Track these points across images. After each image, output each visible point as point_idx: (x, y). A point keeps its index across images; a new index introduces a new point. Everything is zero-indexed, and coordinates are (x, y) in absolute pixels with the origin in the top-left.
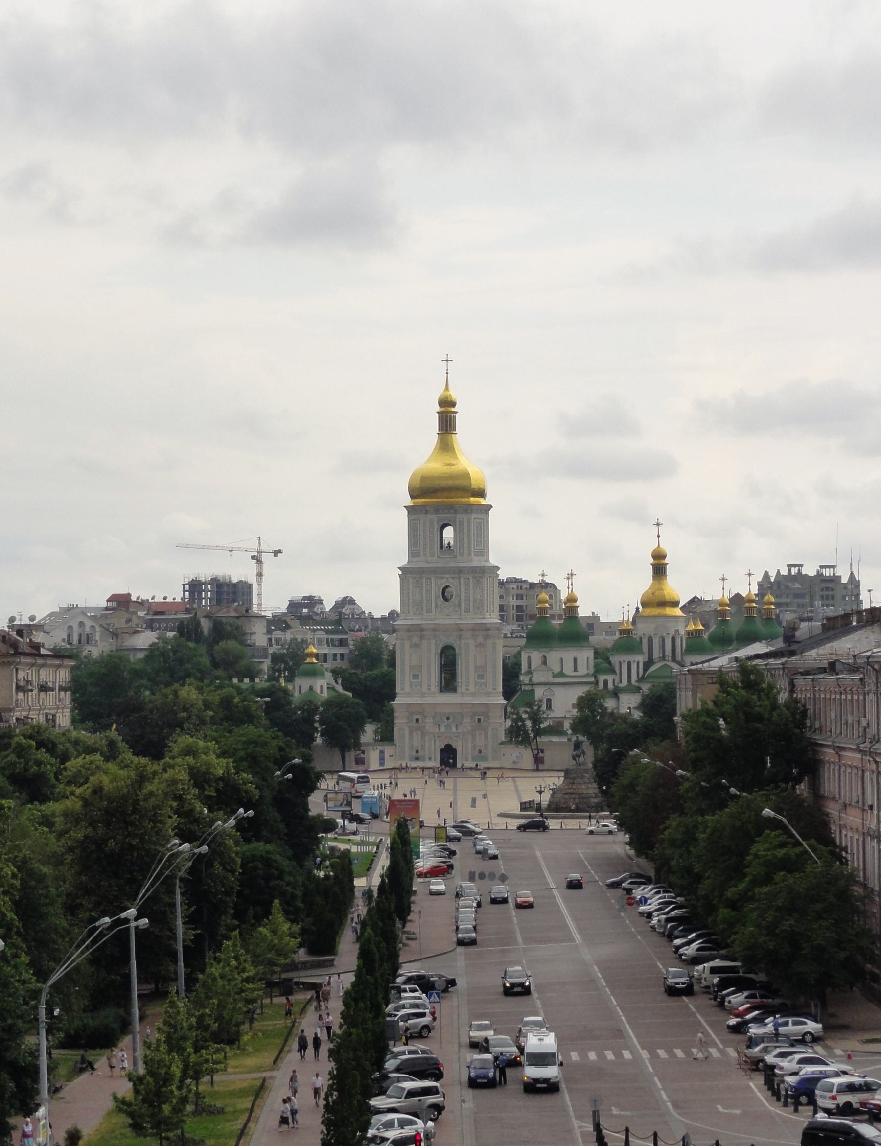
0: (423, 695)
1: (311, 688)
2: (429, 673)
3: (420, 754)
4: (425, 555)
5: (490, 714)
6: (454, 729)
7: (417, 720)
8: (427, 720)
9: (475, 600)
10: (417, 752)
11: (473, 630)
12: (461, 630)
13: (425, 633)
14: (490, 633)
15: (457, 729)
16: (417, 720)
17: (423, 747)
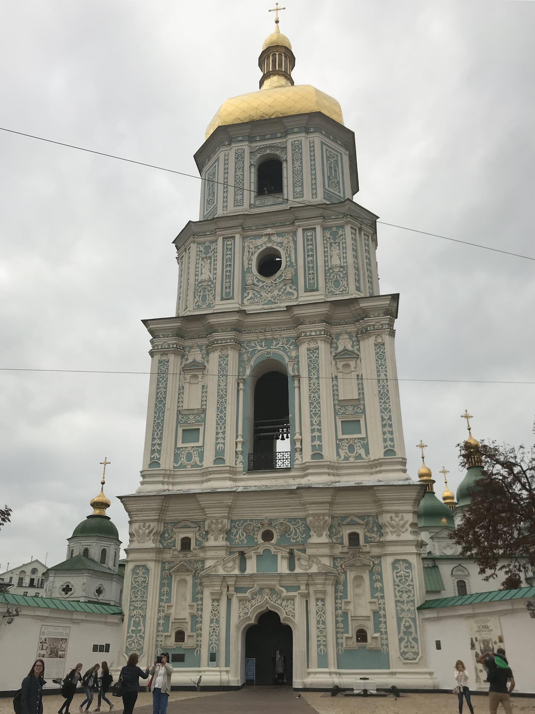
0: (206, 474)
1: (86, 551)
2: (221, 421)
3: (188, 642)
4: (225, 207)
5: (385, 519)
6: (283, 567)
7: (186, 544)
8: (211, 542)
9: (328, 270)
10: (180, 636)
11: (327, 320)
12: (298, 322)
13: (218, 336)
14: (371, 321)
15: (292, 567)
16: (186, 544)
17: (196, 619)
